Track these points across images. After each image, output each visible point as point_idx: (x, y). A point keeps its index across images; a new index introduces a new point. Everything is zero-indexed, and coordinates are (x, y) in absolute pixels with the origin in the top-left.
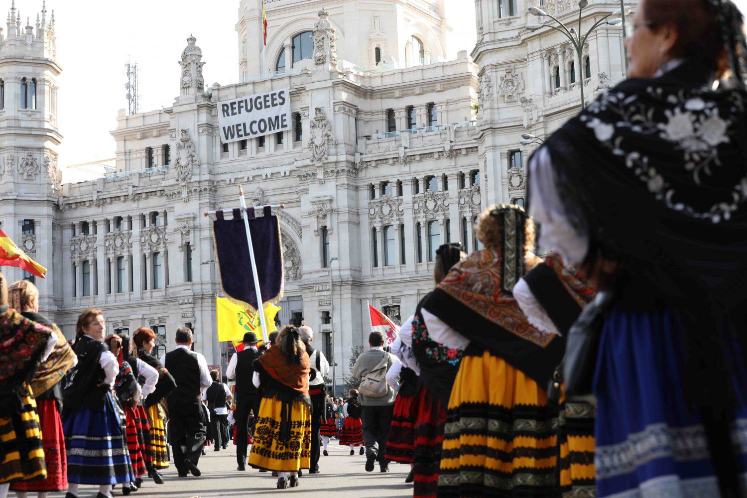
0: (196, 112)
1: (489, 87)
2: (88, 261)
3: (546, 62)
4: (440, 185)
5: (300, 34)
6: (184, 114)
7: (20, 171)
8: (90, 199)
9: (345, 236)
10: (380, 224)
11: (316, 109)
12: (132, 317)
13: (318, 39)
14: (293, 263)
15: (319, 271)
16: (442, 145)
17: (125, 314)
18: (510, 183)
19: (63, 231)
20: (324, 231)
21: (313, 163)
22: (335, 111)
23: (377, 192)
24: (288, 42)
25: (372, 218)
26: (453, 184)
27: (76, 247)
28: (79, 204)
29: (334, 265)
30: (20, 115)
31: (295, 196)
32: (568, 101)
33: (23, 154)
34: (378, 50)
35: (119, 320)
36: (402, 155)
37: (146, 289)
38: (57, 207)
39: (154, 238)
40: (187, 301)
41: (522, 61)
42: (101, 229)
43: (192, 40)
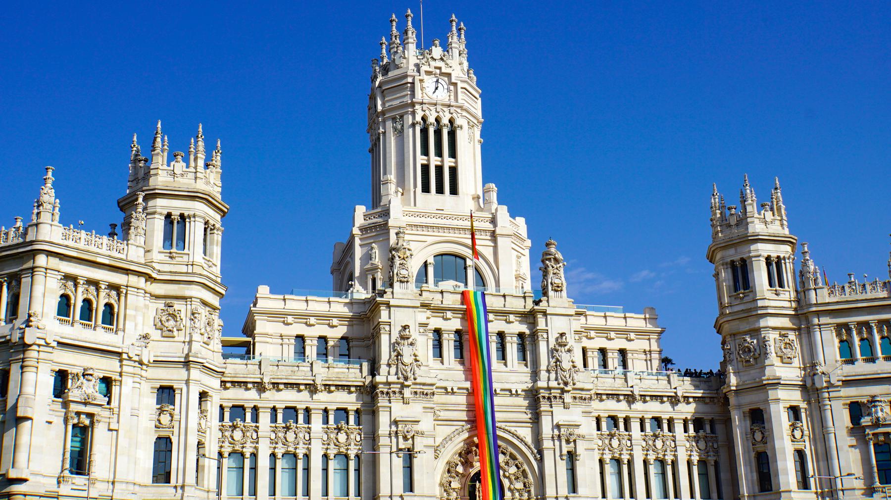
3: (834, 334)
5: (442, 255)
8: (259, 380)
14: (525, 486)
16: (675, 390)
18: (793, 436)
21: (562, 386)
23: (604, 425)
24: (431, 260)
26: (679, 427)
29: (581, 490)
30: (205, 266)
32: (879, 372)
33: (203, 311)
39: (342, 437)
42: (265, 418)
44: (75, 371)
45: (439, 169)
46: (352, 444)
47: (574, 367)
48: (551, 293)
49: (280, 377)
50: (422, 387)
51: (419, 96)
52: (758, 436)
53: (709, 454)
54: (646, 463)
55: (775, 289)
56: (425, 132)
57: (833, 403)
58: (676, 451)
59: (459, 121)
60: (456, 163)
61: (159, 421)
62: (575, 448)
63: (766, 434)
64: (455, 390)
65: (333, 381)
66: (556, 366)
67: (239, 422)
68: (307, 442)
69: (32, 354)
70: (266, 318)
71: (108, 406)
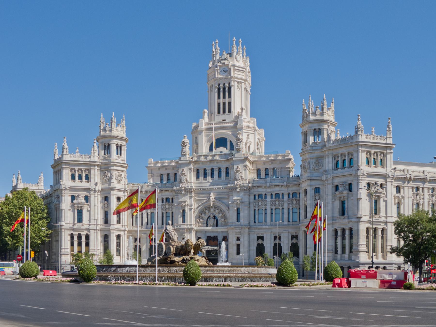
1: (309, 165)
4: (281, 197)
7: (117, 178)
9: (246, 212)
18: (315, 199)
23: (257, 197)
25: (255, 206)
26: (286, 197)
31: (226, 196)
33: (117, 172)
34: (249, 147)
36: (268, 184)
37: (163, 224)
38: (127, 193)
39: (167, 207)
40: (183, 230)
41: (322, 157)
44: (77, 195)
45: (224, 104)
46: (170, 209)
51: (217, 77)
52: (305, 198)
56: (219, 89)
58: (284, 205)
59: (231, 84)
60: (230, 100)
61: (104, 206)
66: (235, 178)
69: (64, 192)
71: (87, 204)
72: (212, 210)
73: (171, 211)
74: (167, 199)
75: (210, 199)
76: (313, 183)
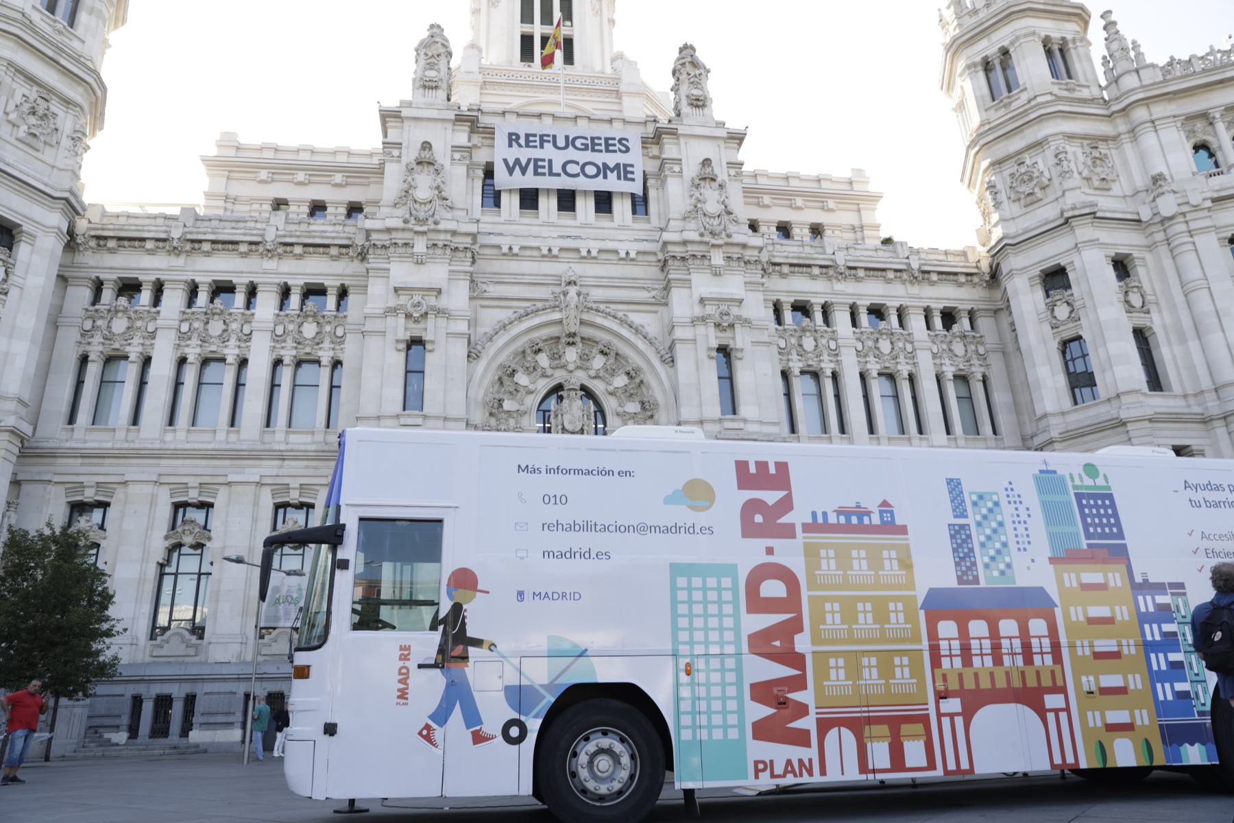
0: (450, 125)
2: (126, 358)
6: (424, 124)
8: (163, 236)
10: (801, 365)
11: (706, 162)
12: (230, 478)
13: (693, 74)
15: (720, 420)
16: (906, 261)
17: (210, 471)
18: (1127, 302)
19: (69, 288)
20: (724, 351)
21: (706, 239)
22: (729, 176)
23: (788, 315)
26: (916, 323)
27: (99, 323)
28: (126, 243)
29: (745, 410)
35: (193, 482)
39: (309, 330)
42: (173, 300)
43: (436, 31)
47: (730, 213)
48: (686, 109)
49: (201, 230)
50: (449, 237)
52: (1062, 312)
53: (972, 362)
54: (863, 377)
55: (1064, 82)
57: (1197, 239)
62: (734, 338)
63: (1077, 305)
64: (516, 250)
65: (298, 236)
67: (123, 301)
68: (245, 338)
70: (227, 173)
72: (571, 355)
73: (331, 353)
74: (314, 291)
75: (565, 294)
76: (1105, 235)
